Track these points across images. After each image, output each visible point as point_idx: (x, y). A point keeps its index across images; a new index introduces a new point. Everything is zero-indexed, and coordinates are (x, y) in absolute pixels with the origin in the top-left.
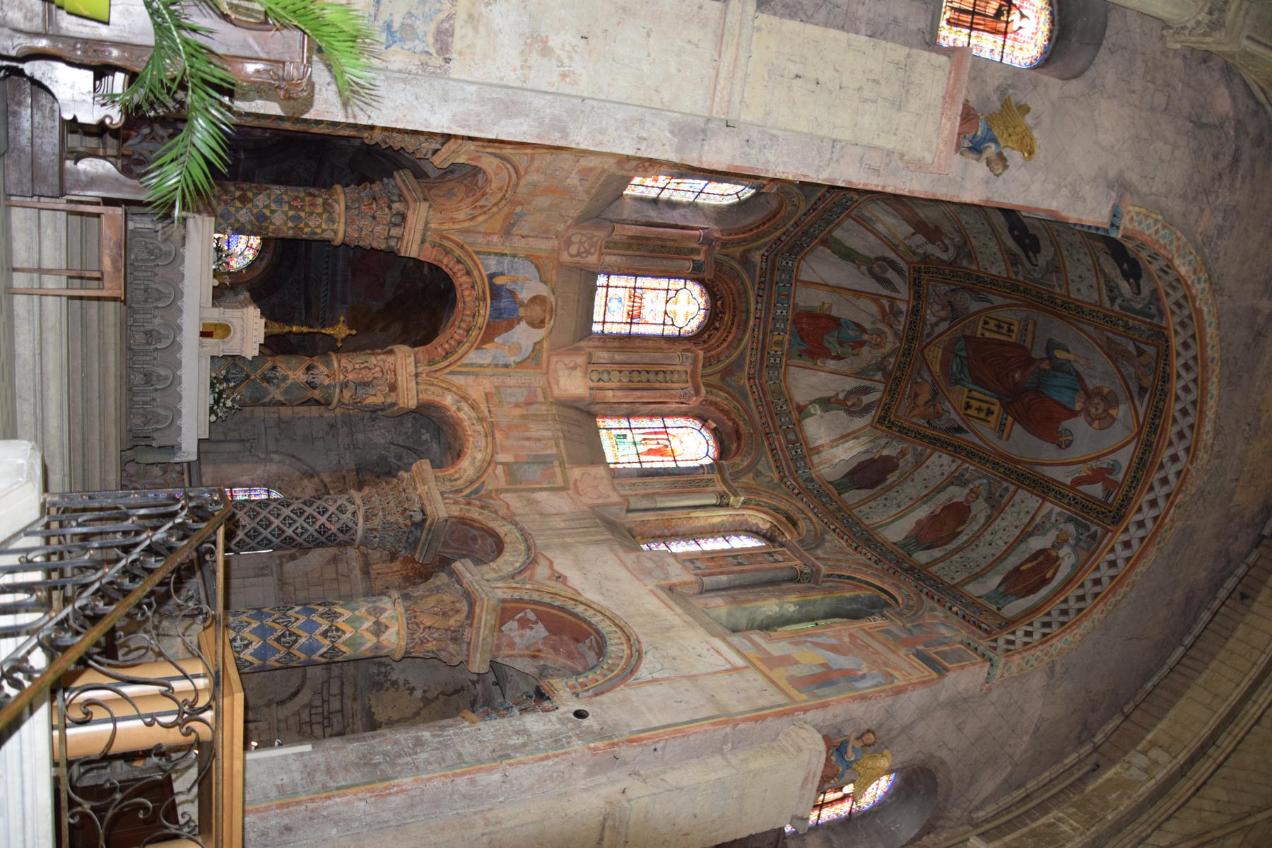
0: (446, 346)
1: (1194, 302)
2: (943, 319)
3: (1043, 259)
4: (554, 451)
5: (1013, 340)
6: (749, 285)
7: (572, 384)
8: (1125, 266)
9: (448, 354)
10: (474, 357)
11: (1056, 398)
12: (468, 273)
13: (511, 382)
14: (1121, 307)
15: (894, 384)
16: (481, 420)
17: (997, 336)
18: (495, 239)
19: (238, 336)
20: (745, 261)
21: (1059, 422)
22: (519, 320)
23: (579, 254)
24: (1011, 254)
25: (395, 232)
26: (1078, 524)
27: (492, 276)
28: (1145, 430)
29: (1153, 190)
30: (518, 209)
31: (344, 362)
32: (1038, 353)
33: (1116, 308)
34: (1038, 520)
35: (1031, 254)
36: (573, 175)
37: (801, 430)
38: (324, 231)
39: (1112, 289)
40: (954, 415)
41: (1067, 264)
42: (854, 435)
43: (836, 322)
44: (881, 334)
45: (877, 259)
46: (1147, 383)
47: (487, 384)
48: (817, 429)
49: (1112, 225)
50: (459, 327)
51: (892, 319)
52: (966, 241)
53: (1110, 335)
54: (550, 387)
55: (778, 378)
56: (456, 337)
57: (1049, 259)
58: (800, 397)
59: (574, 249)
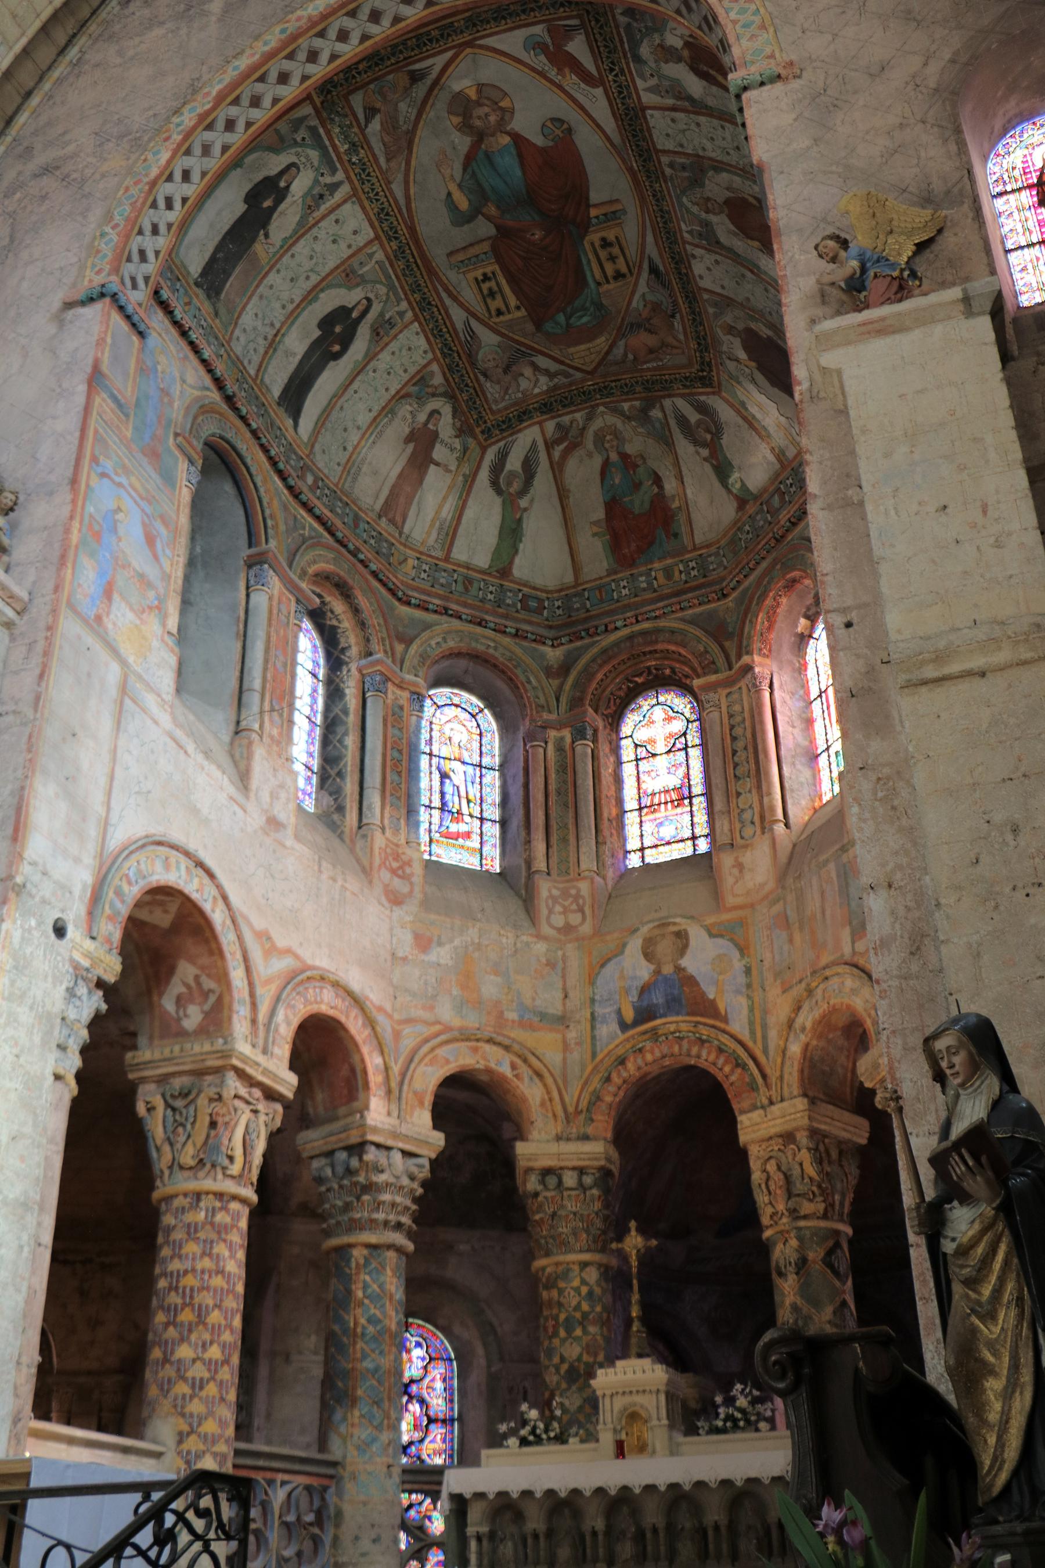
0: (727, 1069)
1: (208, 113)
2: (536, 367)
3: (351, 297)
4: (832, 866)
5: (497, 267)
6: (595, 650)
8: (267, 203)
9: (739, 1064)
10: (739, 1026)
11: (518, 173)
12: (622, 1061)
13: (768, 956)
14: (334, 171)
15: (654, 390)
16: (810, 992)
17: (507, 289)
18: (572, 1035)
19: (639, 1399)
20: (564, 669)
21: (543, 151)
22: (679, 969)
23: (581, 910)
24: (376, 333)
25: (570, 1179)
26: (635, 45)
27: (624, 1026)
28: (460, 40)
29: (75, 260)
30: (512, 1015)
31: (765, 1220)
32: (484, 228)
33: (340, 175)
34: (670, 102)
35: (355, 315)
36: (432, 956)
37: (765, 490)
38: (584, 1282)
39: (316, 198)
40: (642, 287)
41: (331, 264)
42: (741, 410)
43: (612, 506)
44: (599, 439)
45: (499, 491)
46: (403, 79)
47: (774, 992)
48: (756, 469)
49: (103, 295)
50: (699, 1056)
51: (573, 432)
52: (401, 396)
53: (382, 160)
54: (766, 897)
55: (717, 554)
56: (712, 1058)
57: (343, 291)
58: (729, 511)
59: (575, 919)
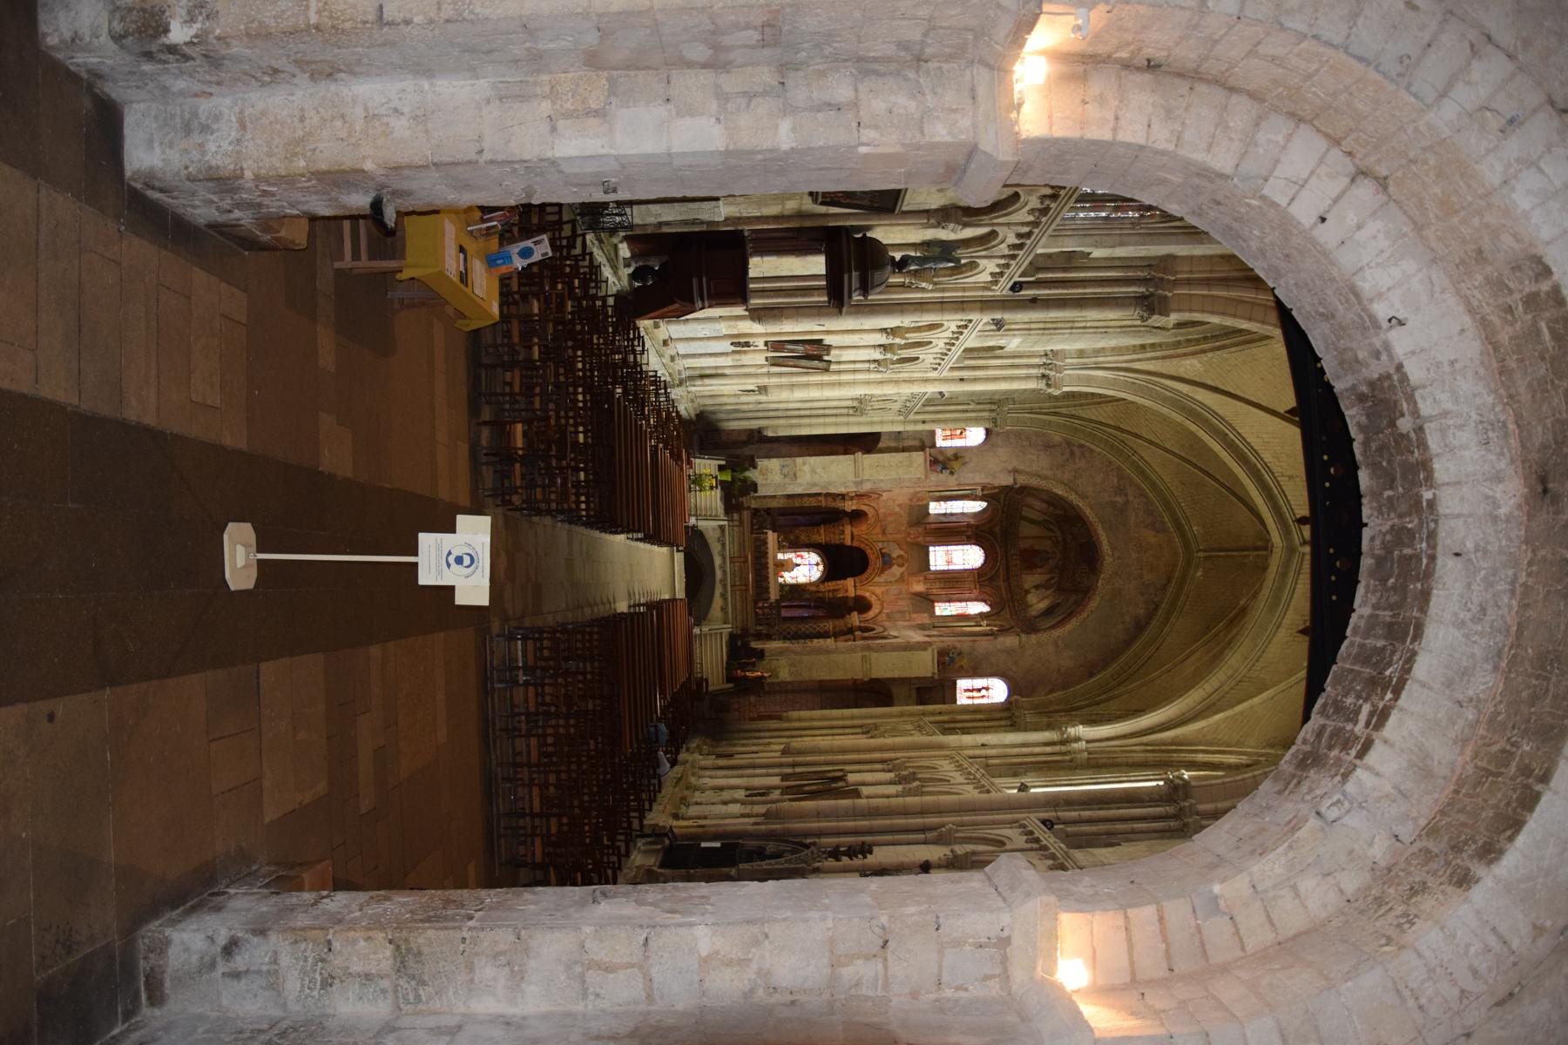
7: (919, 587)
43: (1038, 552)
48: (1032, 598)
58: (1027, 587)
